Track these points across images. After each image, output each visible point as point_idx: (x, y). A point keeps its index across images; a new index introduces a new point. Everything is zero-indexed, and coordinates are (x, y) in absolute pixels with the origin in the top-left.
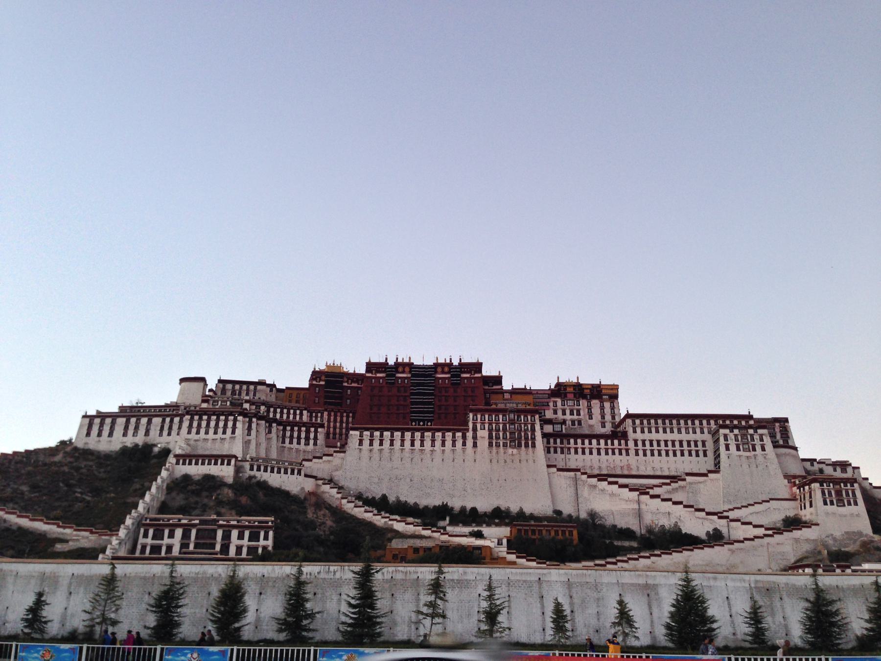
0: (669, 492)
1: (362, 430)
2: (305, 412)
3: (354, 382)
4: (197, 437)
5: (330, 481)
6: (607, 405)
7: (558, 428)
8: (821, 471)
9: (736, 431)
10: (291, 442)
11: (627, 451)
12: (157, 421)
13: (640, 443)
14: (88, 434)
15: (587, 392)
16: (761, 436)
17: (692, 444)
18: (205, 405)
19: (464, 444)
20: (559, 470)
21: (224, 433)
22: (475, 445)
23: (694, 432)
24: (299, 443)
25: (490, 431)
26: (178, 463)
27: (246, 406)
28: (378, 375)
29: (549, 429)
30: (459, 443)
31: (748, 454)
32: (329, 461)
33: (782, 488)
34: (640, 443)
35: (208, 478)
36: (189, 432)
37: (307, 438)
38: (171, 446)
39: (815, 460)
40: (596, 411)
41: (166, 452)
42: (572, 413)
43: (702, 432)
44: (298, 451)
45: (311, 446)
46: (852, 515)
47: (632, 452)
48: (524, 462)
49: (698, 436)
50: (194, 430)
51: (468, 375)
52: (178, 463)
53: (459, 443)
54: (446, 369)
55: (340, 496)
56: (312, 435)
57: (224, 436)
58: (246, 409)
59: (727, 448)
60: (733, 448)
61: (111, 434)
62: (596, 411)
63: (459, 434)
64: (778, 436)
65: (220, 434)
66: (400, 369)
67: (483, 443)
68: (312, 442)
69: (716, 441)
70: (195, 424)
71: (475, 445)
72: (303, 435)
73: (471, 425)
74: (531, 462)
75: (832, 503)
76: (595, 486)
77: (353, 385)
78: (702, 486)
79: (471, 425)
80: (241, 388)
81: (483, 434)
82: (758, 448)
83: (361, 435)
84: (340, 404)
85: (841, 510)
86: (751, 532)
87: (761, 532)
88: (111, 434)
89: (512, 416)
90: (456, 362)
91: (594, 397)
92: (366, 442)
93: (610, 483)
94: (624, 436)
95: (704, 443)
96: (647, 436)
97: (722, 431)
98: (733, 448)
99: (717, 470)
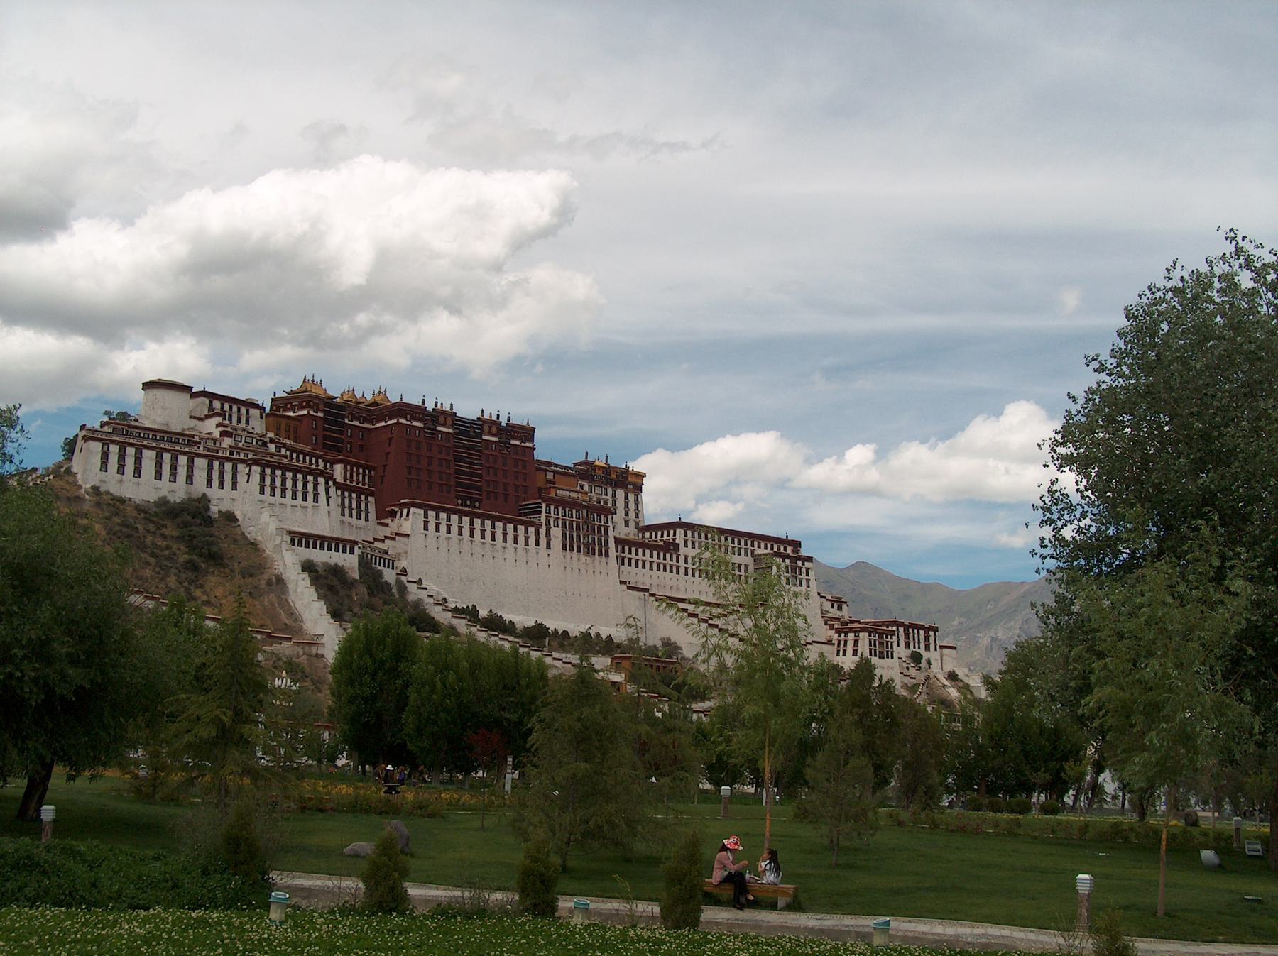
1: (426, 508)
2: (320, 461)
3: (358, 419)
6: (631, 497)
11: (678, 568)
12: (201, 463)
14: (104, 467)
15: (613, 476)
16: (807, 570)
18: (228, 442)
19: (537, 544)
21: (305, 499)
22: (548, 546)
28: (415, 423)
31: (797, 589)
47: (682, 571)
48: (597, 573)
50: (268, 489)
51: (518, 443)
54: (494, 430)
55: (431, 600)
57: (304, 503)
58: (272, 455)
61: (138, 472)
63: (531, 530)
66: (442, 420)
67: (557, 542)
70: (268, 481)
71: (548, 546)
72: (354, 505)
73: (543, 519)
77: (355, 423)
79: (543, 519)
80: (231, 408)
81: (556, 532)
82: (804, 583)
83: (426, 516)
84: (339, 450)
88: (138, 472)
90: (504, 422)
92: (432, 526)
93: (679, 610)
95: (746, 566)
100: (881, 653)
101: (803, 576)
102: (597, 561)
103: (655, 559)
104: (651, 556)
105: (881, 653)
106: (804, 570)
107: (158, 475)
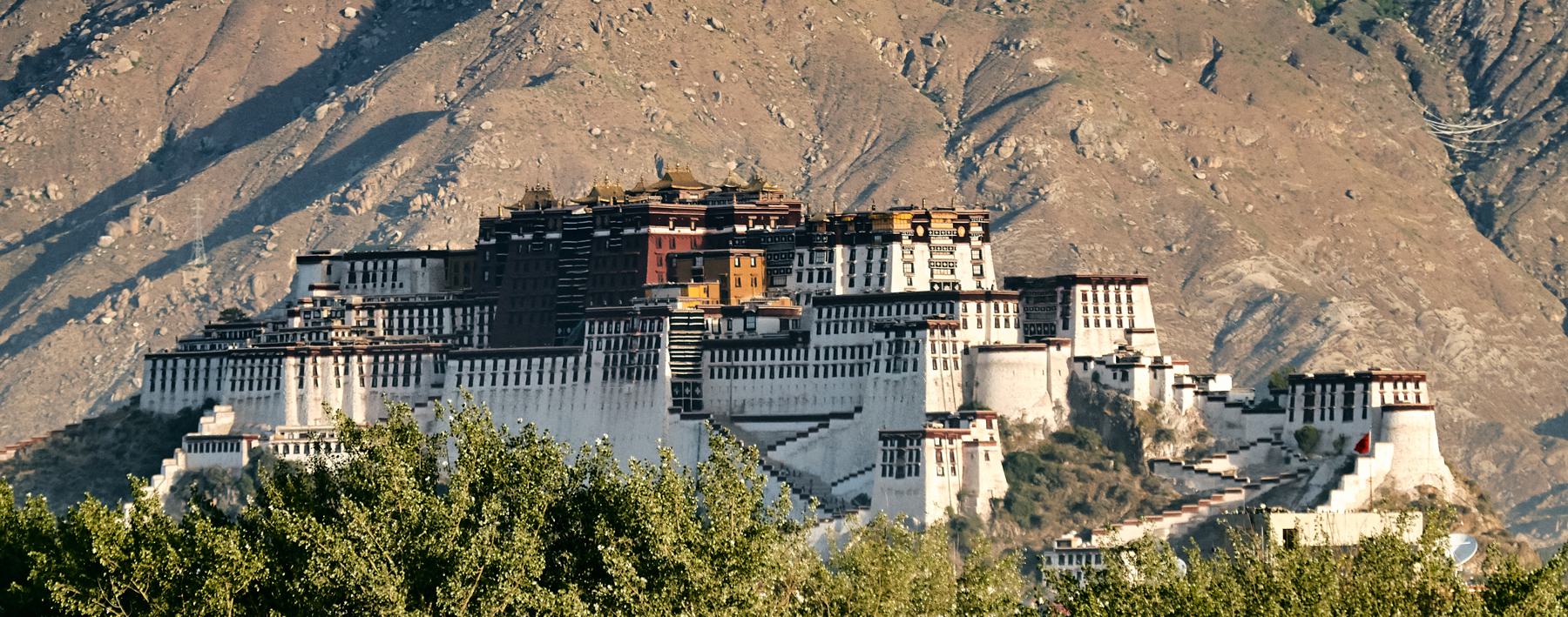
6: (877, 254)
10: (385, 384)
14: (152, 389)
19: (575, 379)
20: (683, 417)
22: (587, 379)
24: (395, 384)
39: (1090, 359)
44: (394, 396)
47: (811, 370)
56: (413, 368)
63: (571, 360)
67: (597, 373)
68: (413, 379)
71: (587, 379)
74: (648, 404)
78: (845, 434)
81: (598, 357)
82: (910, 366)
85: (901, 481)
100: (900, 469)
102: (641, 389)
103: (777, 361)
104: (773, 358)
105: (900, 469)
106: (912, 345)
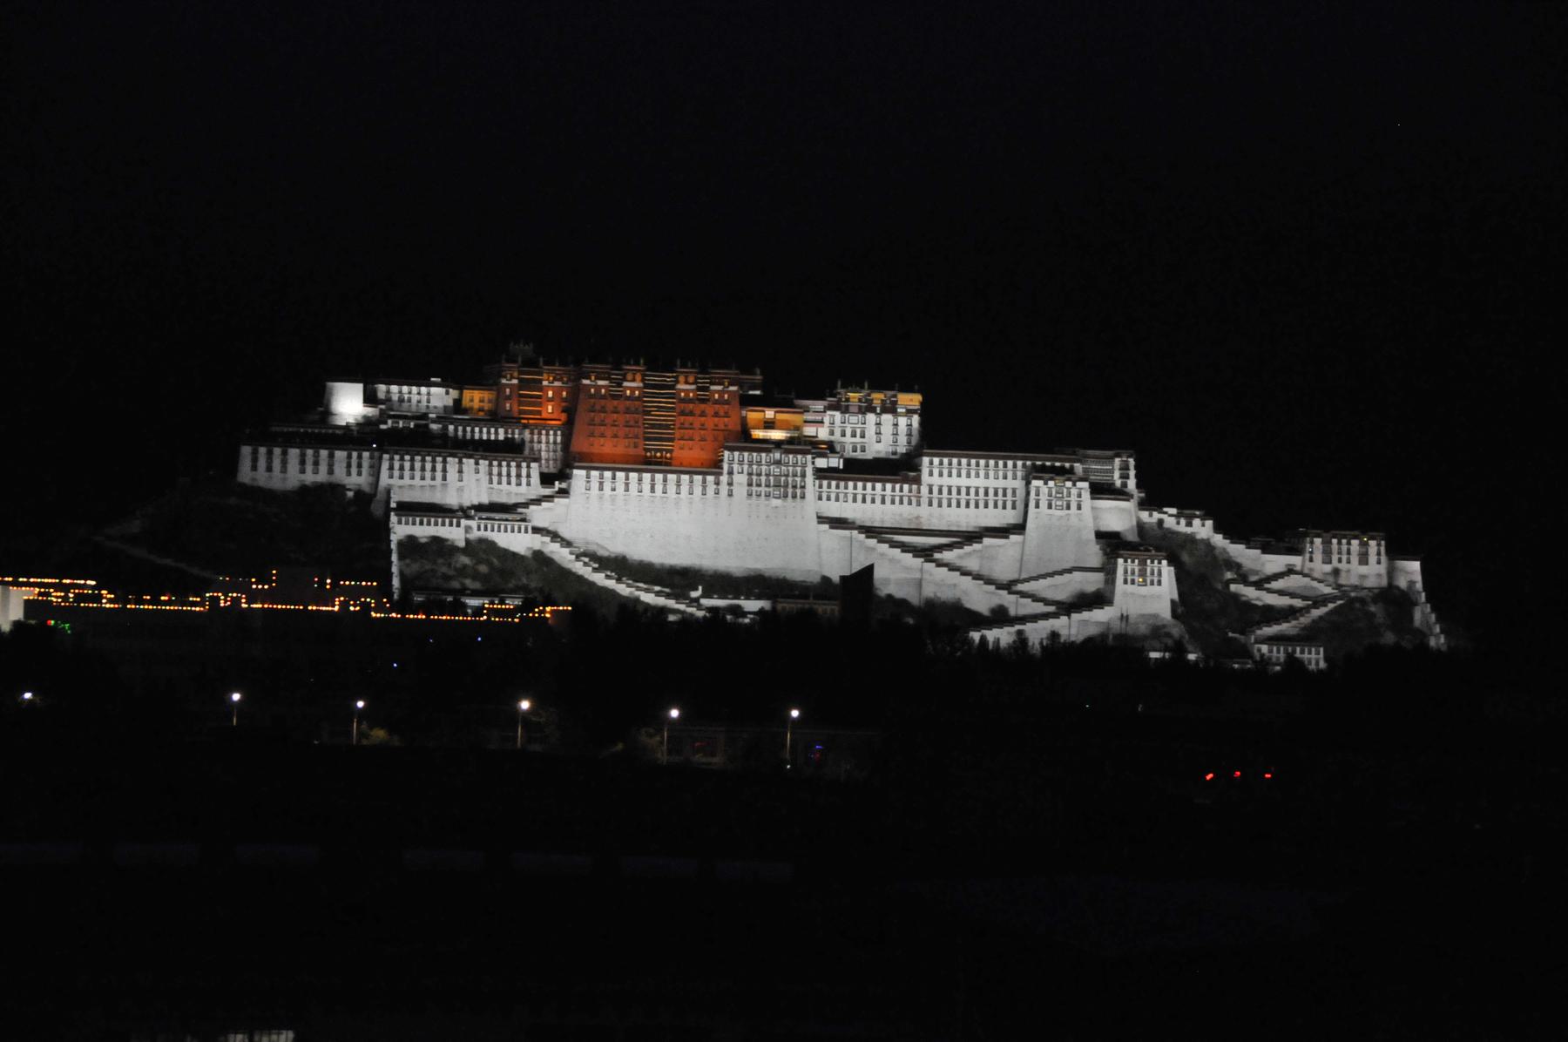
0: (960, 557)
4: (401, 482)
5: (555, 536)
7: (835, 462)
8: (1161, 522)
9: (1051, 483)
13: (935, 490)
15: (877, 403)
17: (1000, 492)
21: (433, 478)
22: (730, 495)
23: (1005, 477)
25: (750, 474)
26: (400, 522)
27: (434, 427)
29: (822, 463)
30: (711, 488)
32: (550, 509)
33: (1094, 555)
34: (935, 490)
35: (437, 541)
36: (391, 477)
37: (519, 476)
38: (367, 489)
40: (887, 429)
41: (364, 498)
42: (854, 435)
43: (1015, 478)
44: (509, 494)
45: (524, 488)
46: (1152, 596)
47: (924, 501)
49: (1010, 483)
52: (400, 522)
53: (711, 488)
54: (691, 379)
59: (1037, 506)
60: (1044, 504)
61: (284, 469)
62: (887, 429)
64: (1117, 474)
65: (428, 481)
66: (629, 376)
67: (740, 489)
68: (524, 480)
69: (1028, 493)
71: (730, 495)
73: (726, 466)
75: (1133, 582)
76: (873, 549)
81: (740, 479)
82: (1074, 506)
83: (588, 477)
86: (1040, 608)
87: (1052, 609)
89: (777, 456)
91: (885, 410)
94: (917, 481)
96: (946, 481)
97: (1035, 483)
98: (1044, 504)
99: (1020, 528)
101: (1074, 498)
106: (1074, 491)
107: (303, 471)
